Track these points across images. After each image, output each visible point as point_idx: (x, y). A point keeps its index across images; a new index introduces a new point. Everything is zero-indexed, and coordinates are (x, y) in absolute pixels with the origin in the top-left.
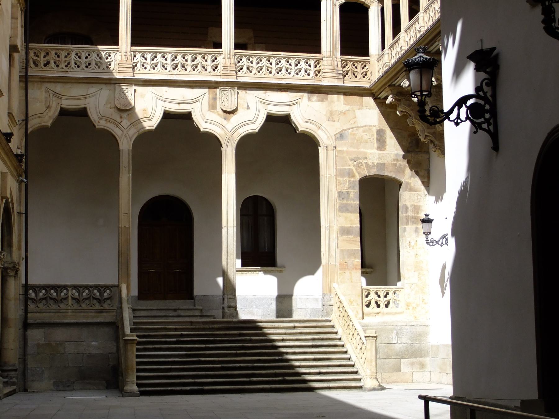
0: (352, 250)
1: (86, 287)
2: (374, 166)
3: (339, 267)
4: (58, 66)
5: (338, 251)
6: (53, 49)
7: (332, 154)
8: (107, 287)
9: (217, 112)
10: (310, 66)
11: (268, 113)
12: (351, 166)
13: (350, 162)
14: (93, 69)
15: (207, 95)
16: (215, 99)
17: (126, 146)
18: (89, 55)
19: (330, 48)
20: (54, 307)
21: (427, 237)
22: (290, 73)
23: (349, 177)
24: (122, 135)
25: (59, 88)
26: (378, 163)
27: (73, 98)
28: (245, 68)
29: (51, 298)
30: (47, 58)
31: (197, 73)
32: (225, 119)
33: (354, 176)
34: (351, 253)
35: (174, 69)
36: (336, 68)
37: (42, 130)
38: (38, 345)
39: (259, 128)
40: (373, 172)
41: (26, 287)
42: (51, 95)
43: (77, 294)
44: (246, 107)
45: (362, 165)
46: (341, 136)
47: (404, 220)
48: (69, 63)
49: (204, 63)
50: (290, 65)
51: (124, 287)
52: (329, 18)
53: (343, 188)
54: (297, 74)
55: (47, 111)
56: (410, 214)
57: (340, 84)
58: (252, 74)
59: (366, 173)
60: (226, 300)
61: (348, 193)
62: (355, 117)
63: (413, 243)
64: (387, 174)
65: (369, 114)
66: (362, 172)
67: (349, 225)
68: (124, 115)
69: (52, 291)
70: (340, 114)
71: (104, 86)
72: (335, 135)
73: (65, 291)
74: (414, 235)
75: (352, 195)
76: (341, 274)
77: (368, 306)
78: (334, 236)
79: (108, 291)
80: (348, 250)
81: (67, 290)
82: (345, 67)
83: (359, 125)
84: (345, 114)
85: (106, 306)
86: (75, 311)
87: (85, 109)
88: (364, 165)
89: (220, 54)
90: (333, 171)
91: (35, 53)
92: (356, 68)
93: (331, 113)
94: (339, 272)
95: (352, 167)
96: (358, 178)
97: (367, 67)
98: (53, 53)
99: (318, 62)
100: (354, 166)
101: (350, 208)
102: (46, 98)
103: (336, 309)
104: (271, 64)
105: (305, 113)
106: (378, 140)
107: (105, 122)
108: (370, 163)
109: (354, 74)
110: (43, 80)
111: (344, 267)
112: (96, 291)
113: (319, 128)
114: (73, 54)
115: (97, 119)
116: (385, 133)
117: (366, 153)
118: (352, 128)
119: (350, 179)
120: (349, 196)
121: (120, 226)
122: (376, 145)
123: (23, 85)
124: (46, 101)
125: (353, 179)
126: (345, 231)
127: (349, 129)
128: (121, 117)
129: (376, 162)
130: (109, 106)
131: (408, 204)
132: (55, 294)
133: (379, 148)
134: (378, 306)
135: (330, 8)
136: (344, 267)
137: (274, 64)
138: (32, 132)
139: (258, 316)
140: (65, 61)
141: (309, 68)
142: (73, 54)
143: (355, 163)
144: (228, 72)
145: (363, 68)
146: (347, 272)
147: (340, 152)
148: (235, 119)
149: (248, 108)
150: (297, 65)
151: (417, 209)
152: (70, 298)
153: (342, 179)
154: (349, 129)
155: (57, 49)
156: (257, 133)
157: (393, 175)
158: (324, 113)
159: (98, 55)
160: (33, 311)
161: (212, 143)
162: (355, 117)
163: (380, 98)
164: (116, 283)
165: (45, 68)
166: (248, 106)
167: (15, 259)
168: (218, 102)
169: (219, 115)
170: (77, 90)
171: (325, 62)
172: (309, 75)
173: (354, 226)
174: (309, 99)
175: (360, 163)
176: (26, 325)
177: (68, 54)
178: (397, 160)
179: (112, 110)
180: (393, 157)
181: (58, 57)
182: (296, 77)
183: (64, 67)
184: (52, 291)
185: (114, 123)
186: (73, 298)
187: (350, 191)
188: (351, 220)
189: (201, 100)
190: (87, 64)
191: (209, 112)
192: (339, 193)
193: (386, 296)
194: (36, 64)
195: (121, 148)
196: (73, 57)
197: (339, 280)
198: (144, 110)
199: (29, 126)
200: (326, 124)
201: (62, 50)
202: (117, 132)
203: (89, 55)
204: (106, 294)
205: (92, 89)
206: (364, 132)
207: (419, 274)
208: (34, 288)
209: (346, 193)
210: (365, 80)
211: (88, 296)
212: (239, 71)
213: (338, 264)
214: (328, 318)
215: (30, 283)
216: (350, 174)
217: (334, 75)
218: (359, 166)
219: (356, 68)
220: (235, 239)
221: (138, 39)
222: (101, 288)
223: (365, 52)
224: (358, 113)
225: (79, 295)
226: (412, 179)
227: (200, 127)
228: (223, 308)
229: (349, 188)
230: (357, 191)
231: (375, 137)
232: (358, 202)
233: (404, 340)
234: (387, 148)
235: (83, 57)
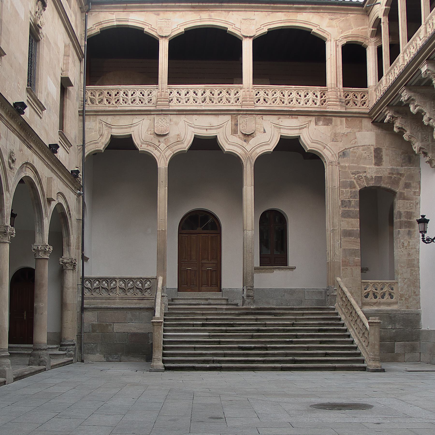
1: (131, 279)
4: (109, 103)
5: (341, 250)
6: (105, 90)
7: (337, 169)
8: (147, 279)
10: (316, 96)
11: (281, 136)
12: (353, 178)
13: (352, 176)
14: (137, 104)
15: (230, 122)
16: (236, 125)
17: (163, 164)
18: (134, 93)
19: (334, 82)
20: (105, 294)
22: (299, 103)
23: (351, 188)
24: (160, 155)
25: (109, 119)
27: (121, 127)
28: (262, 100)
29: (103, 288)
30: (101, 97)
31: (222, 104)
32: (245, 141)
33: (355, 187)
34: (353, 252)
35: (203, 102)
36: (339, 98)
37: (96, 154)
38: (93, 326)
39: (273, 148)
40: (372, 184)
41: (83, 278)
42: (104, 125)
43: (123, 285)
45: (362, 178)
46: (344, 154)
47: (398, 224)
48: (118, 100)
49: (228, 96)
50: (300, 96)
51: (160, 279)
54: (306, 104)
55: (100, 139)
56: (403, 219)
57: (343, 110)
58: (267, 104)
60: (245, 290)
61: (349, 201)
63: (406, 244)
64: (383, 185)
65: (367, 136)
68: (162, 139)
69: (104, 282)
70: (342, 136)
71: (145, 117)
73: (114, 282)
74: (406, 237)
75: (353, 203)
77: (366, 297)
78: (337, 237)
79: (148, 283)
81: (116, 281)
82: (346, 97)
84: (347, 135)
85: (147, 294)
86: (122, 298)
87: (131, 135)
88: (364, 178)
89: (241, 89)
90: (337, 184)
91: (91, 93)
92: (356, 97)
93: (335, 135)
95: (353, 180)
97: (366, 97)
98: (106, 92)
99: (323, 94)
100: (355, 179)
102: (100, 128)
103: (339, 299)
104: (284, 96)
105: (313, 136)
106: (375, 157)
107: (146, 146)
108: (369, 176)
109: (355, 103)
110: (97, 113)
111: (346, 264)
112: (138, 283)
113: (325, 147)
114: (122, 93)
115: (140, 144)
116: (381, 151)
117: (365, 168)
118: (353, 147)
119: (352, 190)
120: (350, 204)
122: (374, 162)
123: (81, 118)
124: (100, 130)
126: (347, 234)
127: (351, 148)
128: (159, 142)
129: (374, 175)
130: (149, 133)
131: (402, 210)
132: (106, 285)
133: (376, 164)
134: (375, 297)
135: (333, 48)
136: (346, 264)
137: (286, 95)
138: (88, 155)
139: (273, 305)
140: (116, 98)
141: (316, 98)
142: (122, 93)
143: (356, 176)
144: (248, 102)
145: (362, 98)
146: (349, 268)
147: (342, 167)
148: (253, 142)
149: (265, 132)
150: (305, 96)
151: (409, 215)
152: (118, 288)
153: (344, 190)
154: (351, 148)
155: (109, 89)
156: (272, 152)
157: (389, 186)
158: (329, 135)
159: (141, 93)
160: (89, 298)
161: (234, 161)
162: (356, 138)
163: (377, 122)
164: (154, 276)
165: (100, 105)
166: (264, 130)
167: (73, 256)
168: (240, 127)
169: (240, 138)
170: (125, 121)
171: (330, 93)
172: (316, 104)
174: (316, 124)
176: (83, 309)
177: (118, 93)
178: (393, 174)
179: (152, 136)
180: (388, 171)
181: (110, 95)
182: (305, 105)
183: (114, 103)
184: (104, 282)
185: (154, 147)
186: (120, 288)
188: (352, 225)
189: (225, 126)
190: (133, 100)
192: (342, 201)
194: (92, 101)
195: (159, 167)
196: (121, 95)
198: (178, 135)
199: (86, 151)
200: (330, 144)
201: (113, 90)
202: (156, 153)
203: (134, 93)
204: (146, 285)
205: (136, 119)
206: (363, 150)
207: (412, 270)
208: (89, 279)
210: (364, 107)
211: (132, 287)
212: (257, 102)
214: (332, 307)
215: (85, 276)
216: (352, 185)
217: (338, 103)
218: (359, 179)
219: (356, 97)
221: (173, 79)
222: (143, 280)
223: (364, 84)
224: (358, 135)
225: (125, 286)
226: (406, 189)
227: (225, 149)
228: (243, 297)
229: (351, 197)
231: (373, 154)
233: (398, 326)
234: (384, 163)
235: (130, 95)
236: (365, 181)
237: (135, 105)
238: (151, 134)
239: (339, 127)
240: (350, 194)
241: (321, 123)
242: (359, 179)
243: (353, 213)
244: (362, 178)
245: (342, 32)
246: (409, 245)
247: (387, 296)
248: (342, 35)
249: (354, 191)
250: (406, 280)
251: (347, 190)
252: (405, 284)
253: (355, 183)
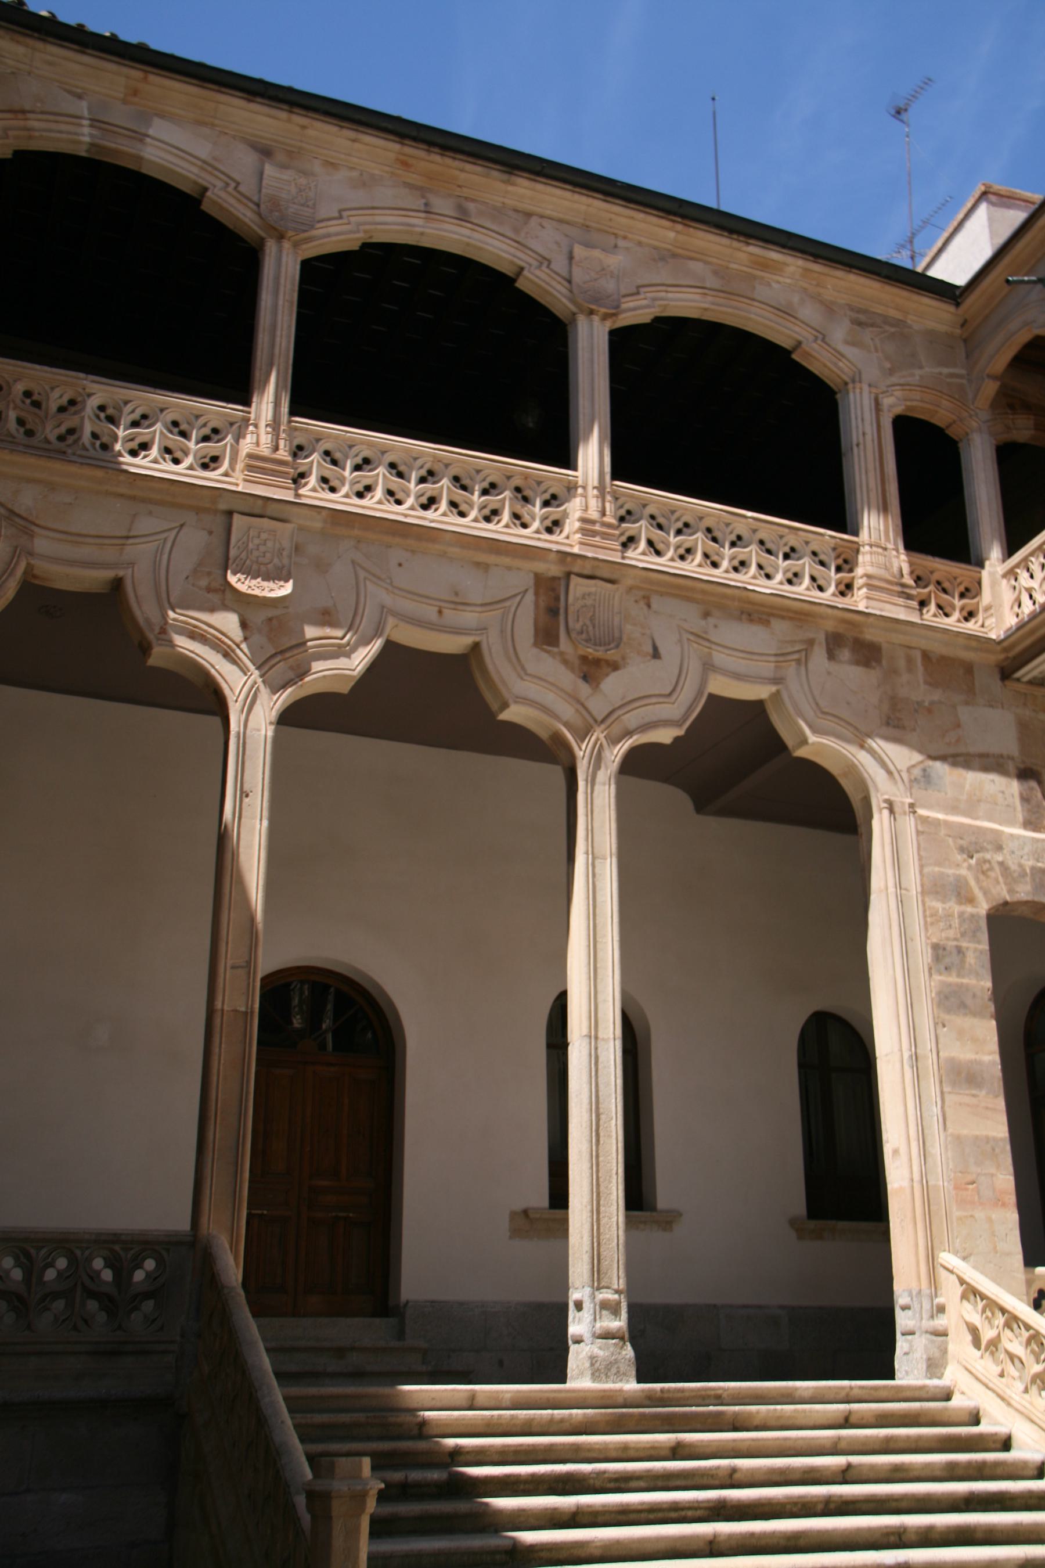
1: (64, 1243)
2: (1023, 874)
4: (30, 433)
7: (908, 825)
8: (146, 1245)
9: (561, 654)
13: (959, 858)
15: (530, 597)
23: (960, 903)
26: (1033, 868)
27: (78, 538)
32: (585, 678)
33: (971, 900)
44: (650, 650)
45: (991, 869)
52: (869, 437)
53: (947, 935)
59: (1002, 893)
61: (959, 950)
62: (959, 726)
66: (994, 891)
70: (916, 711)
72: (909, 770)
75: (971, 959)
76: (960, 1219)
79: (150, 1264)
80: (977, 1138)
83: (972, 750)
84: (929, 711)
88: (997, 868)
94: (956, 1213)
95: (963, 872)
96: (983, 907)
100: (970, 867)
101: (969, 1001)
112: (98, 1263)
119: (963, 908)
120: (963, 961)
121: (218, 1005)
122: (1020, 817)
125: (969, 909)
126: (961, 1076)
129: (1028, 863)
130: (204, 582)
146: (979, 1214)
147: (925, 820)
149: (656, 654)
153: (938, 905)
163: (1018, 680)
166: (655, 649)
169: (565, 662)
173: (987, 1058)
174: (831, 656)
175: (985, 861)
187: (964, 944)
191: (535, 651)
192: (935, 947)
209: (955, 952)
218: (983, 870)
220: (620, 1082)
224: (965, 713)
229: (963, 934)
230: (987, 947)
232: (988, 984)
236: (1001, 879)
237: (144, 462)
238: (209, 590)
239: (905, 677)
240: (960, 925)
241: (845, 654)
242: (983, 873)
243: (974, 996)
244: (991, 869)
245: (891, 372)
248: (894, 379)
249: (972, 916)
251: (947, 906)
253: (972, 883)
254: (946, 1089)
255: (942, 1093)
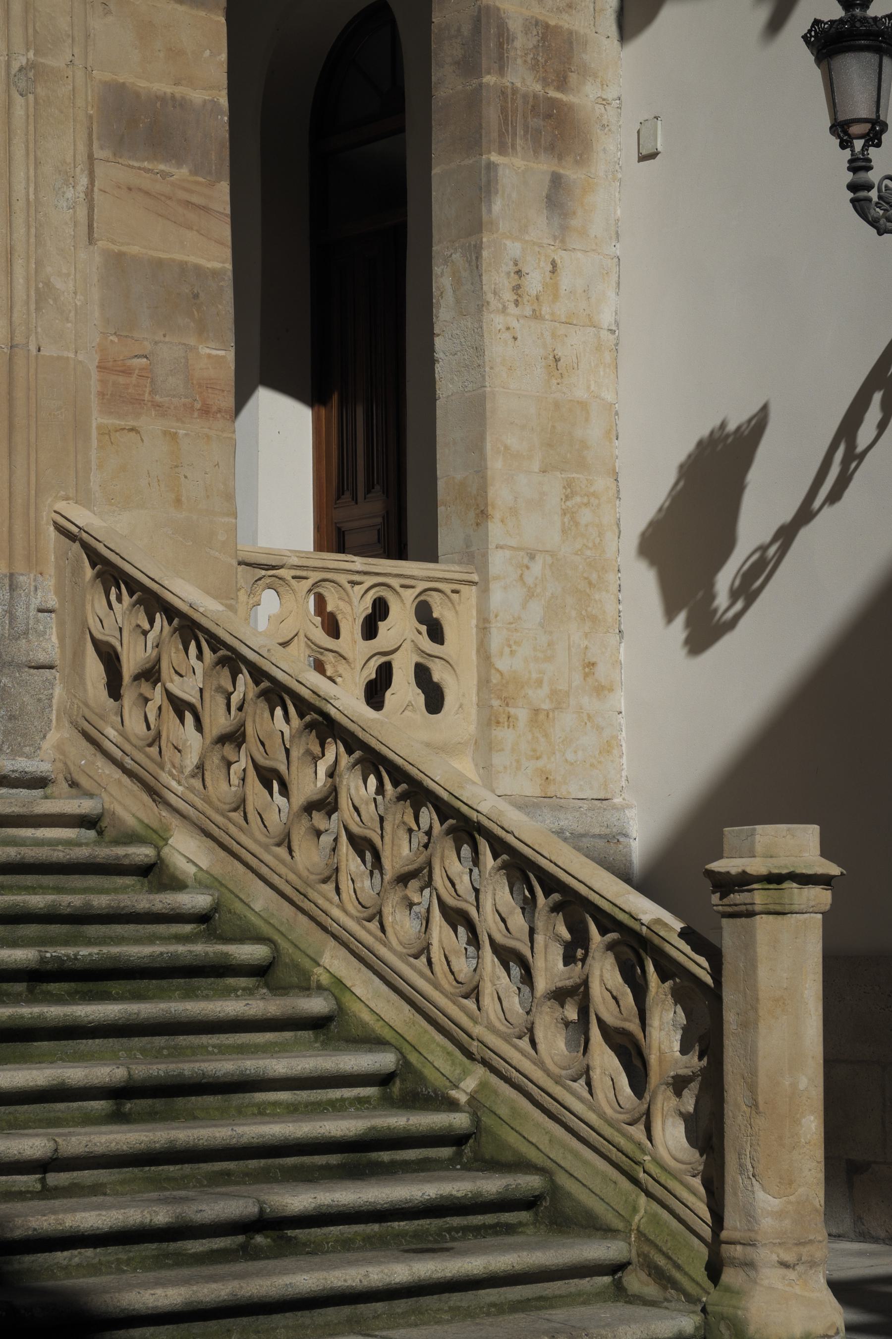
0: (183, 267)
3: (94, 385)
21: (859, 165)
56: (520, 78)
63: (534, 282)
67: (164, 88)
74: (540, 227)
76: (105, 432)
80: (159, 264)
94: (97, 419)
146: (151, 424)
173: (197, 96)
193: (370, 630)
197: (95, 480)
207: (570, 490)
213: (90, 360)
246: (553, 289)
247: (403, 690)
250: (537, 568)
252: (531, 594)
254: (98, 154)
255: (91, 157)
